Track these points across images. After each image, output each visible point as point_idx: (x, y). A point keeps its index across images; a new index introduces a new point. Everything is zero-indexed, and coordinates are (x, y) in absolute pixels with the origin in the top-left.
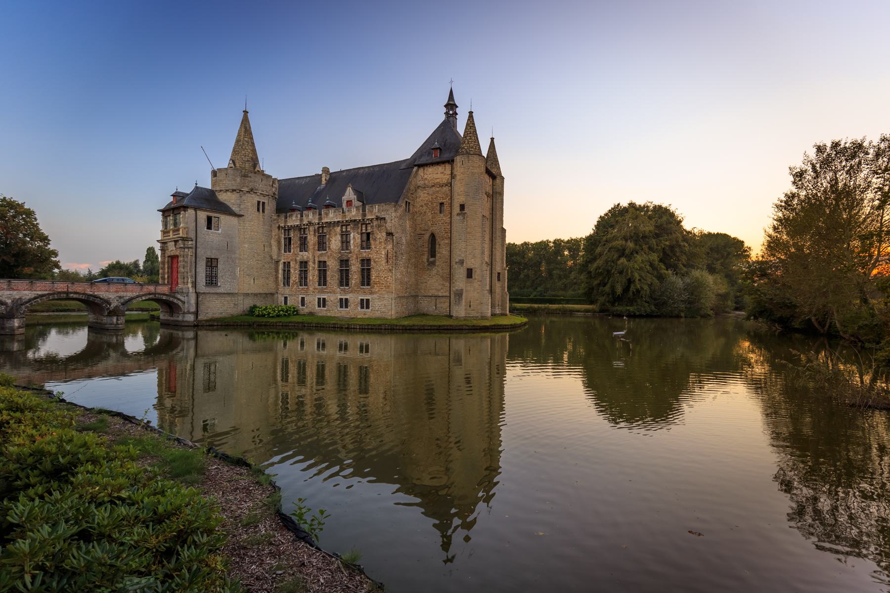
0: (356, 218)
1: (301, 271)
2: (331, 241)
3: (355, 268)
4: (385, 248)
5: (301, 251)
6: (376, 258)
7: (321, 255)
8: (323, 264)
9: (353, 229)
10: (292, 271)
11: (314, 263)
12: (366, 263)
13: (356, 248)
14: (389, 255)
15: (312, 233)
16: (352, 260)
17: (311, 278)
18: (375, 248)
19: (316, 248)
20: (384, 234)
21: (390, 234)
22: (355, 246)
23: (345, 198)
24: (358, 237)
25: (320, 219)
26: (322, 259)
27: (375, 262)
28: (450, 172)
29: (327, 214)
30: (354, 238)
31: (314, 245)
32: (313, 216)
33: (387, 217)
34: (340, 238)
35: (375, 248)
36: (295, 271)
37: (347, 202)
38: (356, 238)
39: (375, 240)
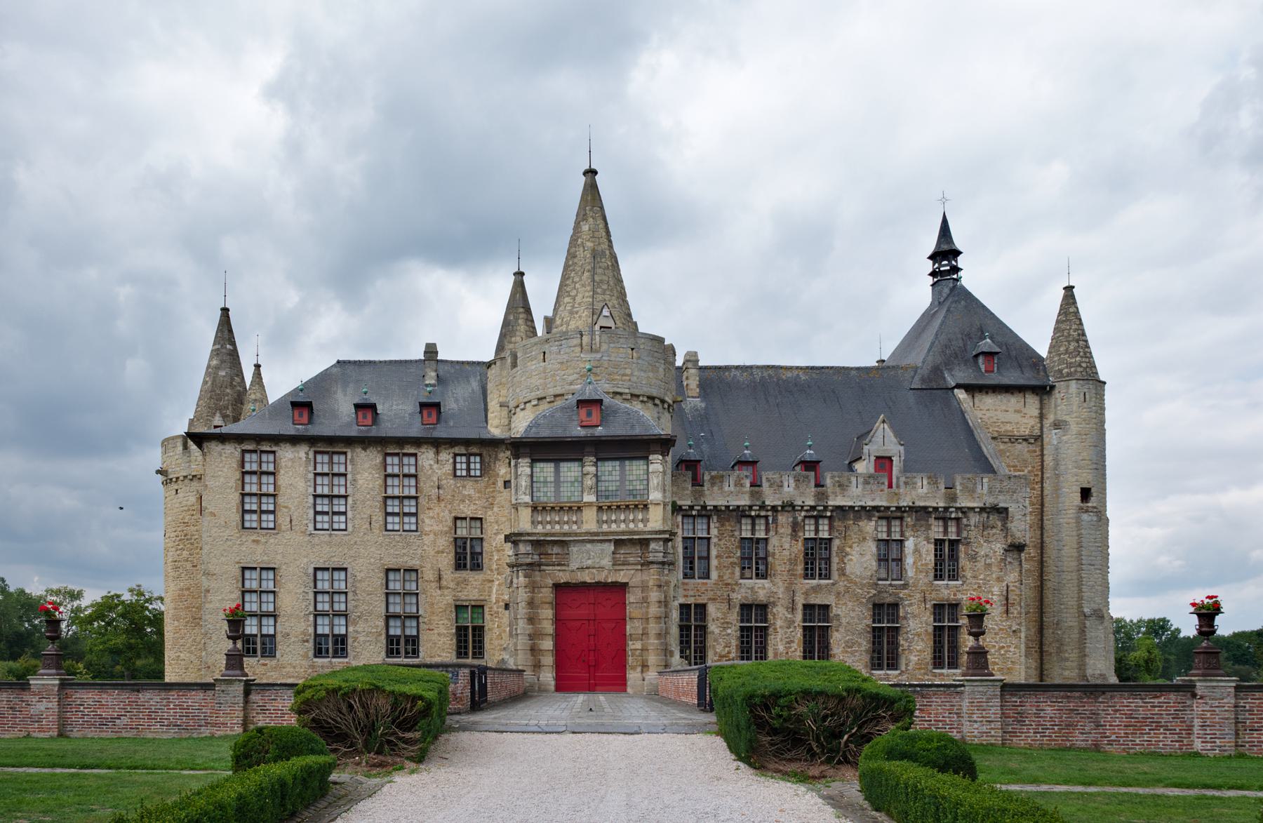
0: (927, 504)
1: (742, 629)
2: (847, 554)
4: (999, 579)
5: (742, 578)
7: (816, 589)
10: (713, 627)
13: (921, 576)
14: (1011, 597)
16: (911, 605)
17: (781, 648)
19: (800, 569)
20: (999, 547)
21: (1017, 548)
22: (918, 571)
25: (822, 496)
29: (842, 486)
30: (917, 551)
31: (792, 561)
32: (797, 487)
34: (874, 549)
37: (878, 458)
38: (924, 551)
39: (973, 558)
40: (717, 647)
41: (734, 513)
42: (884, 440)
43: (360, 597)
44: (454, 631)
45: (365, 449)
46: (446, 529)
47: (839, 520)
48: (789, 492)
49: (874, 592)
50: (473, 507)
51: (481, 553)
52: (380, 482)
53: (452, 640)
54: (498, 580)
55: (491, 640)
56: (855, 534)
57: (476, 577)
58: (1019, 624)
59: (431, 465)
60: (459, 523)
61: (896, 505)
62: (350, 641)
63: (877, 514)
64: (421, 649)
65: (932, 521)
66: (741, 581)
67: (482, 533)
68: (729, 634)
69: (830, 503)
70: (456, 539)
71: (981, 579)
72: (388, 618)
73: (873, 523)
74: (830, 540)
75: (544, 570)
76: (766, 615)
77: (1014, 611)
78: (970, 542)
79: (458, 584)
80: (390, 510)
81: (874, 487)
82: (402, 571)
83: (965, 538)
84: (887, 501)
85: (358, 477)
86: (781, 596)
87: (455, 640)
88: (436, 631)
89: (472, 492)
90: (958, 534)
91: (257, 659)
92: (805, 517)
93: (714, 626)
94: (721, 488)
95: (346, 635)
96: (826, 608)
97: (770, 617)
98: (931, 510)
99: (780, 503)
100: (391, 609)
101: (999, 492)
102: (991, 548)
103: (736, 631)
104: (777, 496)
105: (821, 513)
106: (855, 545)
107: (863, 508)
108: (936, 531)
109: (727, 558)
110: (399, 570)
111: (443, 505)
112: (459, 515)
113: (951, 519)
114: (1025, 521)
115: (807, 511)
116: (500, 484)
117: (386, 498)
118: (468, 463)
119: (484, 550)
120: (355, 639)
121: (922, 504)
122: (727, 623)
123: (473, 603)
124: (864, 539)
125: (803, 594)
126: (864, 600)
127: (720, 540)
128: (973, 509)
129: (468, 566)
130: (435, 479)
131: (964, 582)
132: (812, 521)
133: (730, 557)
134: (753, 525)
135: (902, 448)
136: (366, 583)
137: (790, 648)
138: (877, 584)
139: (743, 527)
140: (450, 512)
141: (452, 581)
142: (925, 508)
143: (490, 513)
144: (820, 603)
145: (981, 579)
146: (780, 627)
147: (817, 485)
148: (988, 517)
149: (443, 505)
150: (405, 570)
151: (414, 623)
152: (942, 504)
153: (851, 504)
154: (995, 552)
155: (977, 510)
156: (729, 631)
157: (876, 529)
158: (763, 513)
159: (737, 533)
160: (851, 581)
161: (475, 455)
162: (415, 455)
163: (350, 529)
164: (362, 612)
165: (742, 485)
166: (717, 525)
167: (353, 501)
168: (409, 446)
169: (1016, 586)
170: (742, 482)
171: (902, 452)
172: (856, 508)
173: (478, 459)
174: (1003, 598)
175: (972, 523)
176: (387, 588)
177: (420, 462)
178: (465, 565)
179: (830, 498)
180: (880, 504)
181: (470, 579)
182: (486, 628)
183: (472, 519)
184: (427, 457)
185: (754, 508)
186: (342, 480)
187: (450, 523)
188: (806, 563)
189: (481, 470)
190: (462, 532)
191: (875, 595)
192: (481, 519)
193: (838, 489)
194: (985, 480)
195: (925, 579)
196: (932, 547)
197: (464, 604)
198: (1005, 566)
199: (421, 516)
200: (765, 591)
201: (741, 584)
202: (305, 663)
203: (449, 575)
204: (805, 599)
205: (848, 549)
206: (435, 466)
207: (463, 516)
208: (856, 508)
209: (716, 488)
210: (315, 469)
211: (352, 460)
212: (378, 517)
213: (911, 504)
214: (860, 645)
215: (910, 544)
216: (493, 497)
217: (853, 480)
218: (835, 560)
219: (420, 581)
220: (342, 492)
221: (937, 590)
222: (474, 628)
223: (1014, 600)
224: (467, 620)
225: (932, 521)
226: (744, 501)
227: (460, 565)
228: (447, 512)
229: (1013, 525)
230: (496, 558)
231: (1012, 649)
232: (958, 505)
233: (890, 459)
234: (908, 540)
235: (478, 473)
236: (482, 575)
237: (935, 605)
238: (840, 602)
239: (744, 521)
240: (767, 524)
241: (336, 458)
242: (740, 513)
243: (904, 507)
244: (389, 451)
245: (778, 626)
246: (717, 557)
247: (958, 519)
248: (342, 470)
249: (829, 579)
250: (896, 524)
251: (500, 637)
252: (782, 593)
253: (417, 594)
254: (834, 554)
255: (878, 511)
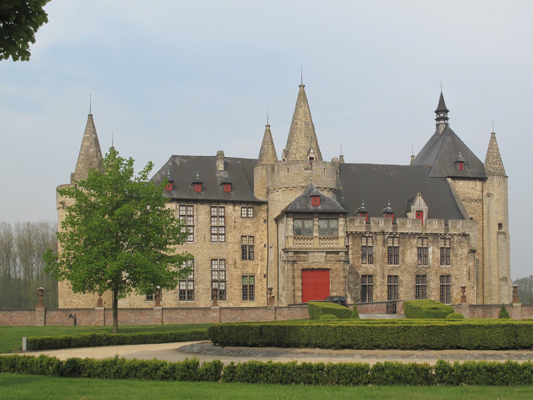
0: (438, 232)
2: (405, 253)
3: (434, 284)
4: (466, 265)
6: (457, 275)
7: (393, 269)
8: (393, 279)
9: (432, 242)
11: (384, 278)
12: (445, 278)
14: (471, 272)
15: (380, 243)
16: (431, 276)
17: (379, 295)
18: (456, 264)
19: (386, 260)
20: (466, 251)
21: (473, 251)
23: (415, 207)
24: (438, 252)
25: (395, 228)
26: (393, 273)
27: (456, 278)
28: (480, 189)
29: (404, 224)
30: (433, 252)
31: (383, 257)
32: (385, 224)
33: (471, 234)
34: (416, 252)
35: (456, 264)
36: (356, 286)
37: (417, 211)
38: (436, 252)
39: (456, 256)
40: (353, 294)
41: (359, 235)
42: (420, 204)
43: (200, 272)
44: (242, 287)
45: (202, 204)
46: (238, 241)
47: (402, 239)
48: (382, 226)
49: (417, 270)
50: (250, 231)
51: (253, 252)
52: (209, 219)
53: (240, 292)
54: (261, 264)
55: (258, 291)
56: (409, 245)
57: (251, 263)
58: (474, 284)
59: (231, 212)
60: (243, 238)
61: (425, 232)
62: (195, 292)
63: (417, 236)
64: (227, 296)
65: (439, 239)
66: (362, 265)
67: (253, 243)
68: (357, 288)
69: (399, 231)
70: (242, 245)
71: (459, 265)
72: (213, 281)
73: (416, 240)
74: (398, 247)
75: (298, 263)
76: (372, 280)
77: (472, 279)
78: (454, 249)
79: (243, 266)
80: (213, 232)
81: (417, 225)
82: (218, 260)
83: (453, 247)
84: (422, 231)
85: (199, 217)
86: (378, 272)
87: (242, 292)
88: (234, 288)
89: (249, 224)
90: (450, 245)
91: (153, 301)
92: (389, 237)
93: (351, 285)
94: (354, 224)
95: (193, 290)
96: (397, 276)
97: (374, 281)
98: (439, 235)
99: (378, 231)
100: (214, 278)
101: (466, 227)
102: (463, 251)
103: (360, 287)
104: (377, 228)
105: (395, 236)
106: (408, 250)
107: (412, 233)
108: (442, 244)
109: (356, 254)
110: (217, 260)
111: (236, 230)
112: (244, 235)
113: (447, 238)
114: (476, 240)
115: (388, 234)
116: (262, 220)
117: (211, 227)
118: (247, 211)
119: (254, 251)
120: (198, 292)
121: (435, 232)
122: (357, 283)
123: (250, 275)
124: (412, 247)
125: (388, 271)
126: (413, 274)
127: (353, 247)
128: (455, 234)
129: (248, 258)
130: (233, 218)
131: (452, 266)
132: (391, 239)
133: (357, 254)
134: (367, 240)
135: (427, 207)
136: (203, 266)
137: (382, 294)
138: (418, 267)
139: (363, 241)
140: (240, 234)
141: (241, 265)
142: (436, 234)
143: (257, 234)
144: (395, 275)
145: (459, 265)
146: (378, 285)
147: (393, 224)
148: (461, 238)
149: (236, 230)
150: (220, 260)
151: (224, 284)
152: (443, 233)
153: (407, 232)
154: (464, 253)
155: (457, 235)
156: (357, 287)
157: (417, 243)
158: (371, 235)
159: (360, 244)
160: (407, 265)
161: (250, 208)
162: (224, 207)
163: (195, 240)
164: (201, 279)
165: (363, 223)
166: (352, 240)
167: (197, 228)
168: (222, 203)
169: (472, 268)
170: (363, 221)
171: (427, 209)
172: (409, 234)
173: (252, 210)
174: (468, 273)
175: (455, 240)
176: (212, 268)
177: (226, 211)
178: (246, 257)
179: (399, 229)
180: (419, 232)
181: (249, 264)
182: (255, 286)
183: (250, 236)
184: (229, 208)
185: (367, 233)
186: (192, 219)
187: (240, 237)
188: (389, 257)
189: (253, 214)
190: (245, 243)
191: (417, 271)
192: (253, 237)
193: (402, 226)
194: (460, 222)
195: (437, 265)
196: (439, 250)
197: (246, 275)
198: (468, 259)
199: (227, 235)
200: (372, 270)
201: (362, 266)
202: (175, 303)
203: (239, 262)
204: (388, 273)
205: (406, 251)
206: (233, 213)
207: (245, 235)
208: (409, 234)
209: (351, 224)
210: (179, 213)
211: (196, 209)
212: (208, 235)
213: (431, 232)
214: (411, 293)
215: (430, 249)
216: (259, 227)
217: (408, 221)
218: (400, 256)
219: (227, 265)
220: (192, 224)
221: (442, 269)
222: (250, 286)
223: (472, 274)
224: (247, 282)
225: (439, 239)
226: (363, 230)
227: (244, 258)
228: (238, 233)
229: (471, 241)
230: (260, 254)
231: (471, 295)
232: (450, 233)
233: (422, 212)
234: (430, 247)
235: (252, 216)
236: (254, 262)
237: (441, 276)
238: (403, 274)
239: (363, 239)
240: (373, 240)
241: (189, 208)
242: (362, 235)
243: (428, 233)
244: (213, 206)
245: (377, 285)
246: (352, 254)
247: (449, 239)
248: (192, 213)
249: (398, 264)
250: (425, 240)
251: (261, 290)
252: (380, 270)
253: (225, 271)
254: (400, 253)
255: (418, 235)
